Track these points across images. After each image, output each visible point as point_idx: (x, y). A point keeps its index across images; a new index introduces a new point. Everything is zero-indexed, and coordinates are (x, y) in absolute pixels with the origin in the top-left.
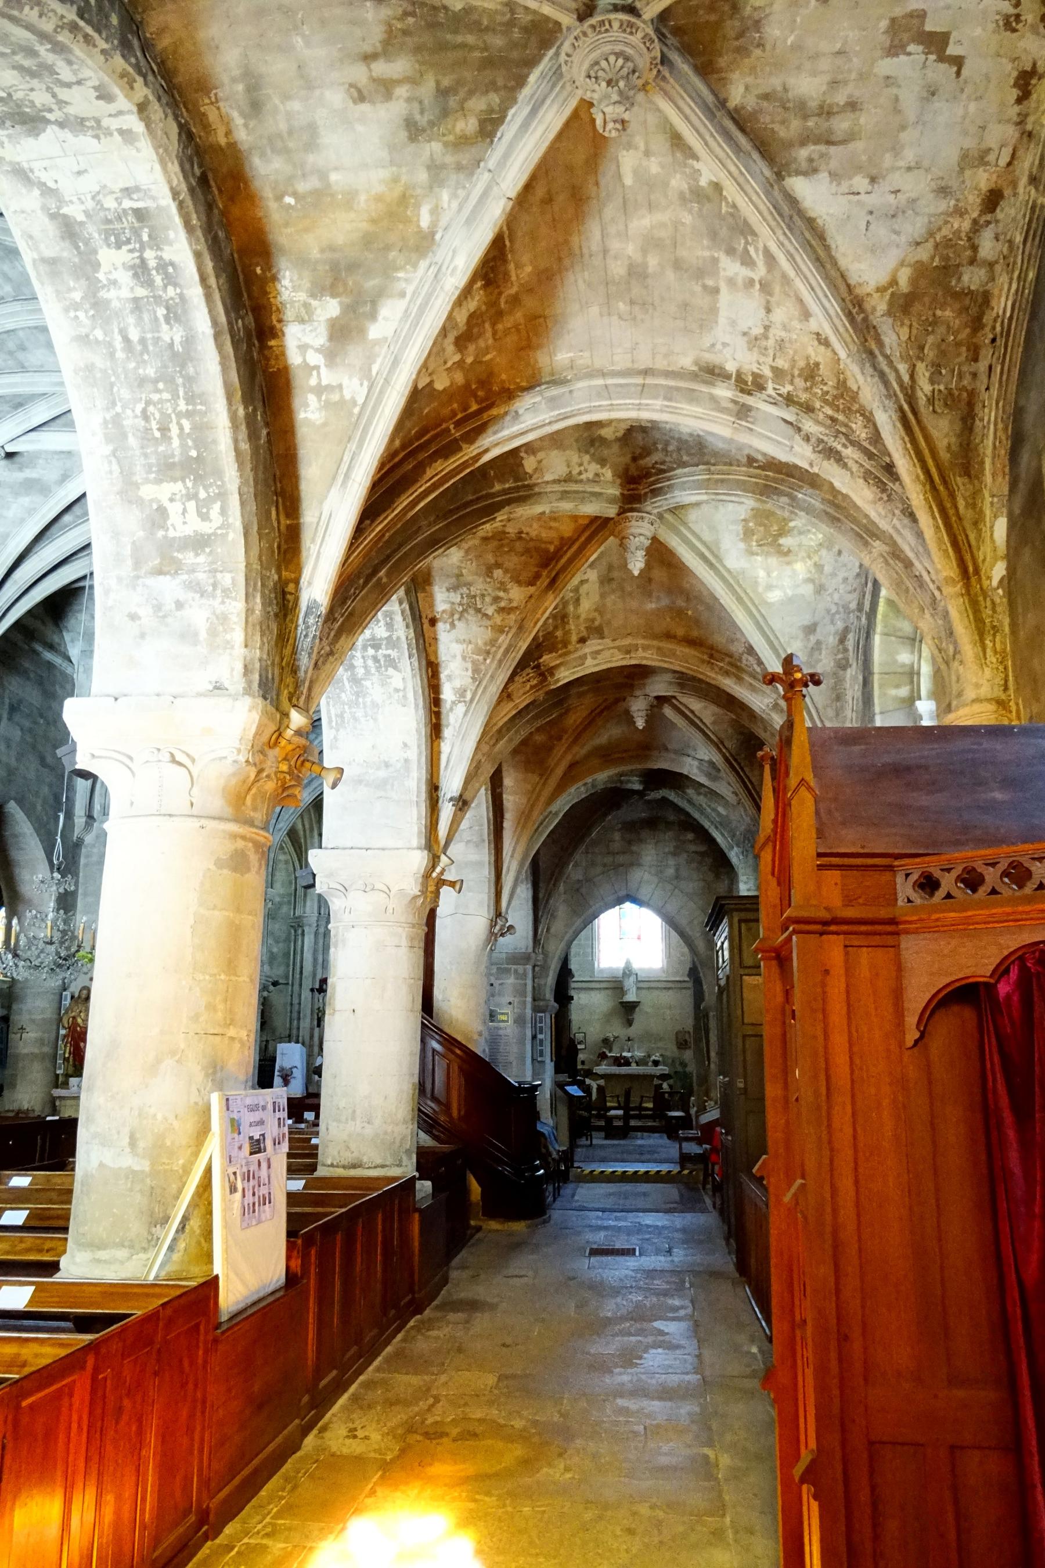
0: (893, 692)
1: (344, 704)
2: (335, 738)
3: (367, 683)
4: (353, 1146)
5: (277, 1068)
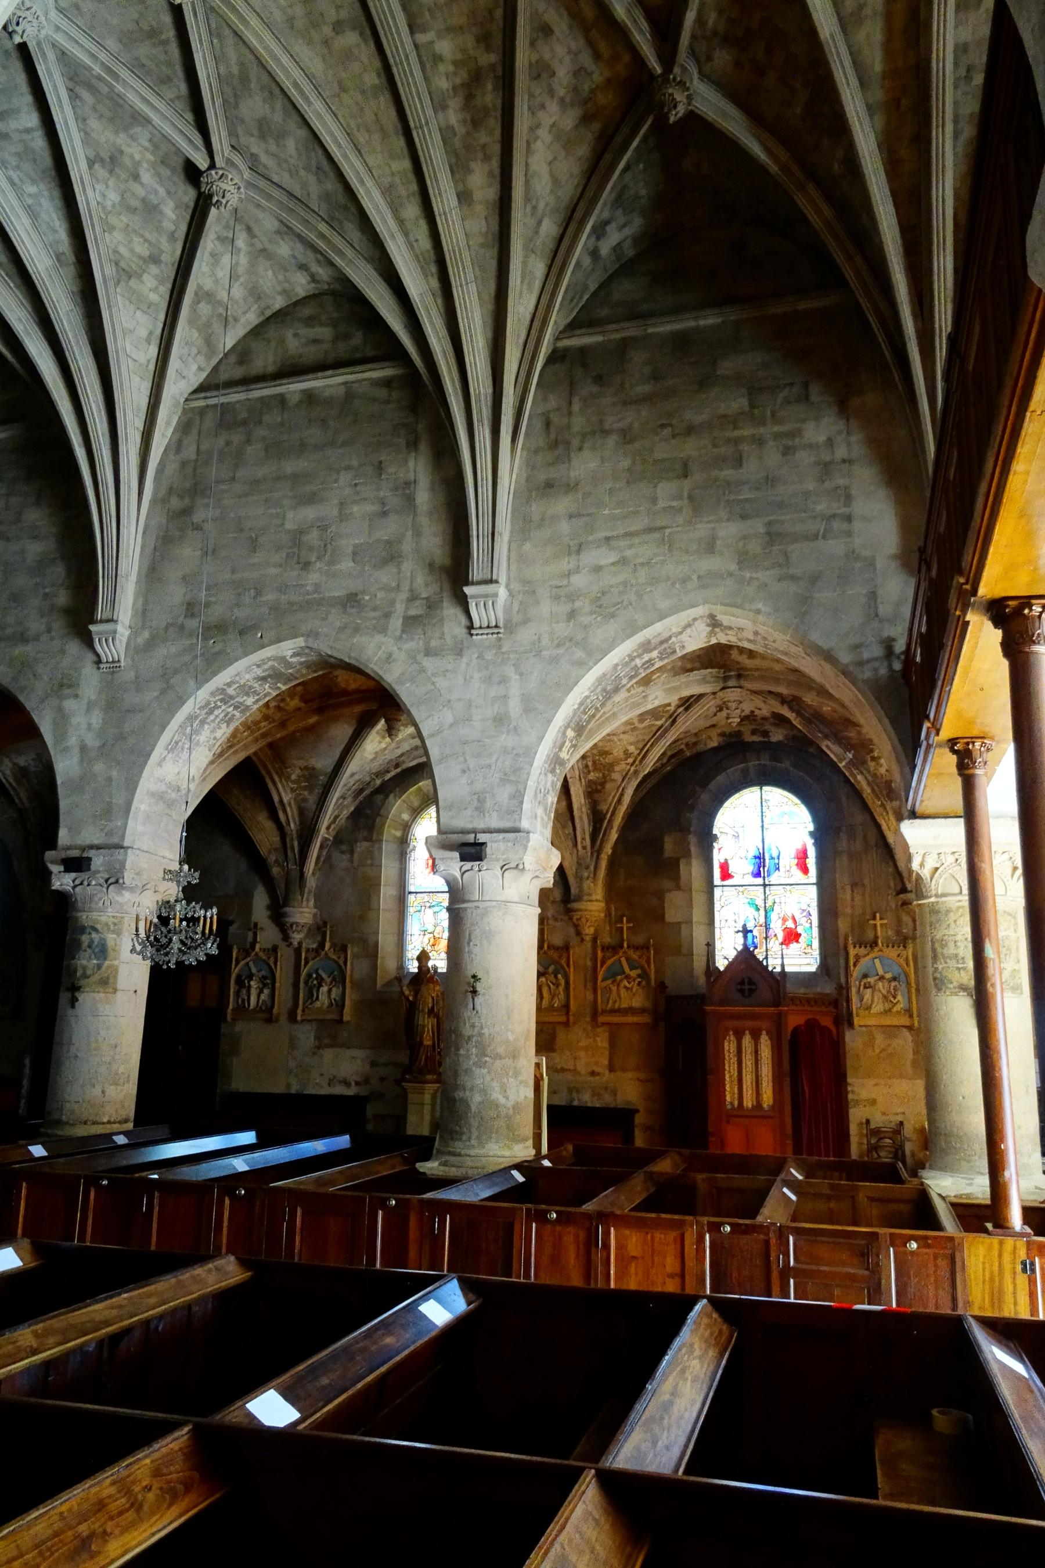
0: (393, 832)
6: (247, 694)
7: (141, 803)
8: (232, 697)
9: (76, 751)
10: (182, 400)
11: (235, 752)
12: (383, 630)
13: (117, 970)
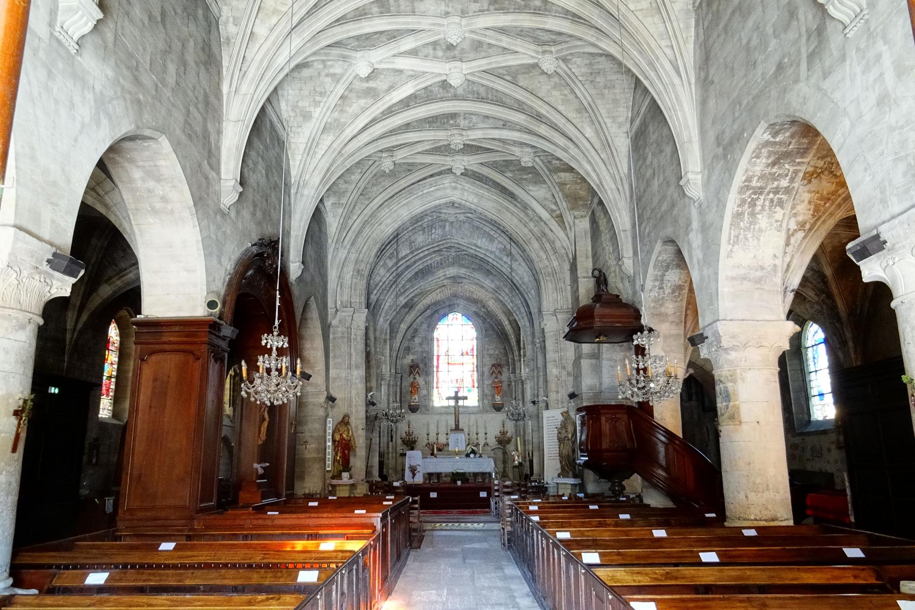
1: (741, 229)
2: (731, 251)
3: (760, 216)
4: (770, 507)
5: (407, 466)
6: (775, 179)
7: (725, 288)
8: (761, 188)
9: (696, 266)
10: (690, 7)
11: (824, 222)
12: (797, 81)
13: (738, 408)
